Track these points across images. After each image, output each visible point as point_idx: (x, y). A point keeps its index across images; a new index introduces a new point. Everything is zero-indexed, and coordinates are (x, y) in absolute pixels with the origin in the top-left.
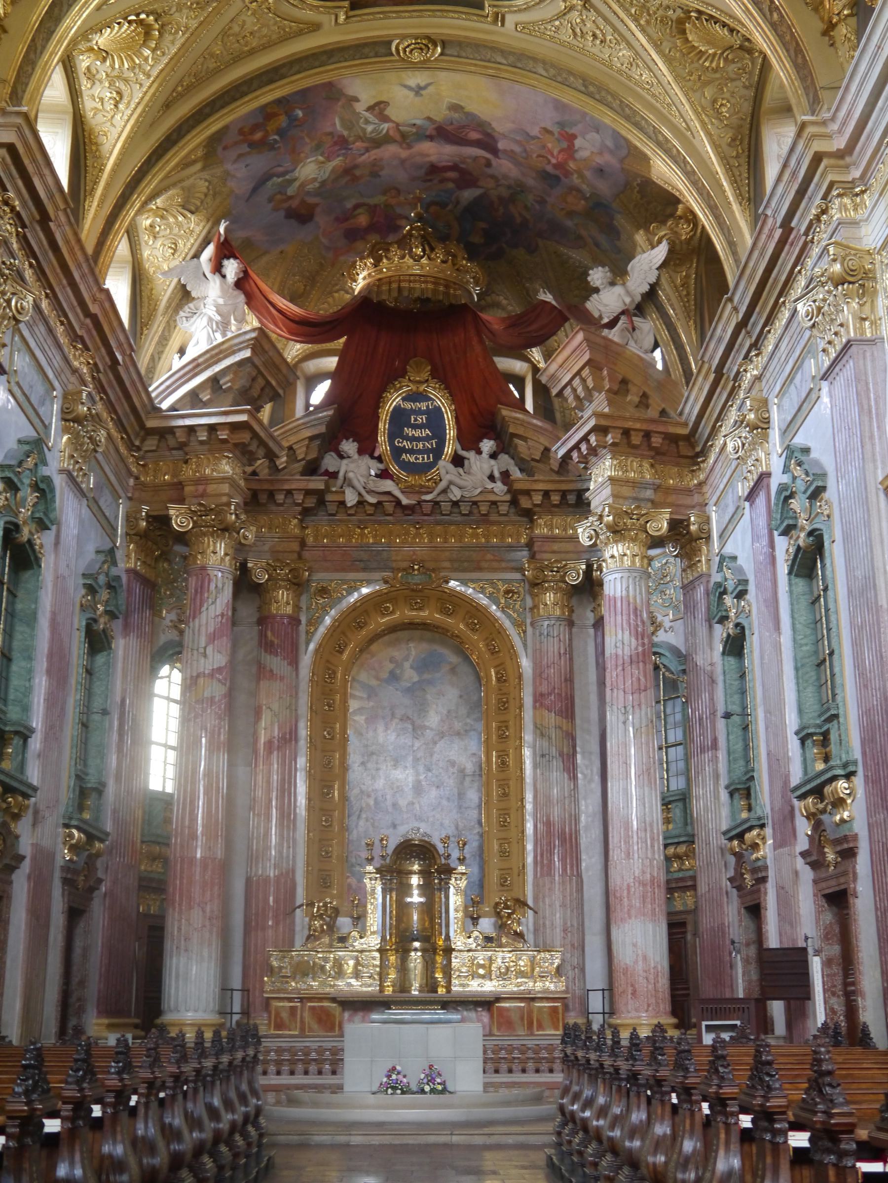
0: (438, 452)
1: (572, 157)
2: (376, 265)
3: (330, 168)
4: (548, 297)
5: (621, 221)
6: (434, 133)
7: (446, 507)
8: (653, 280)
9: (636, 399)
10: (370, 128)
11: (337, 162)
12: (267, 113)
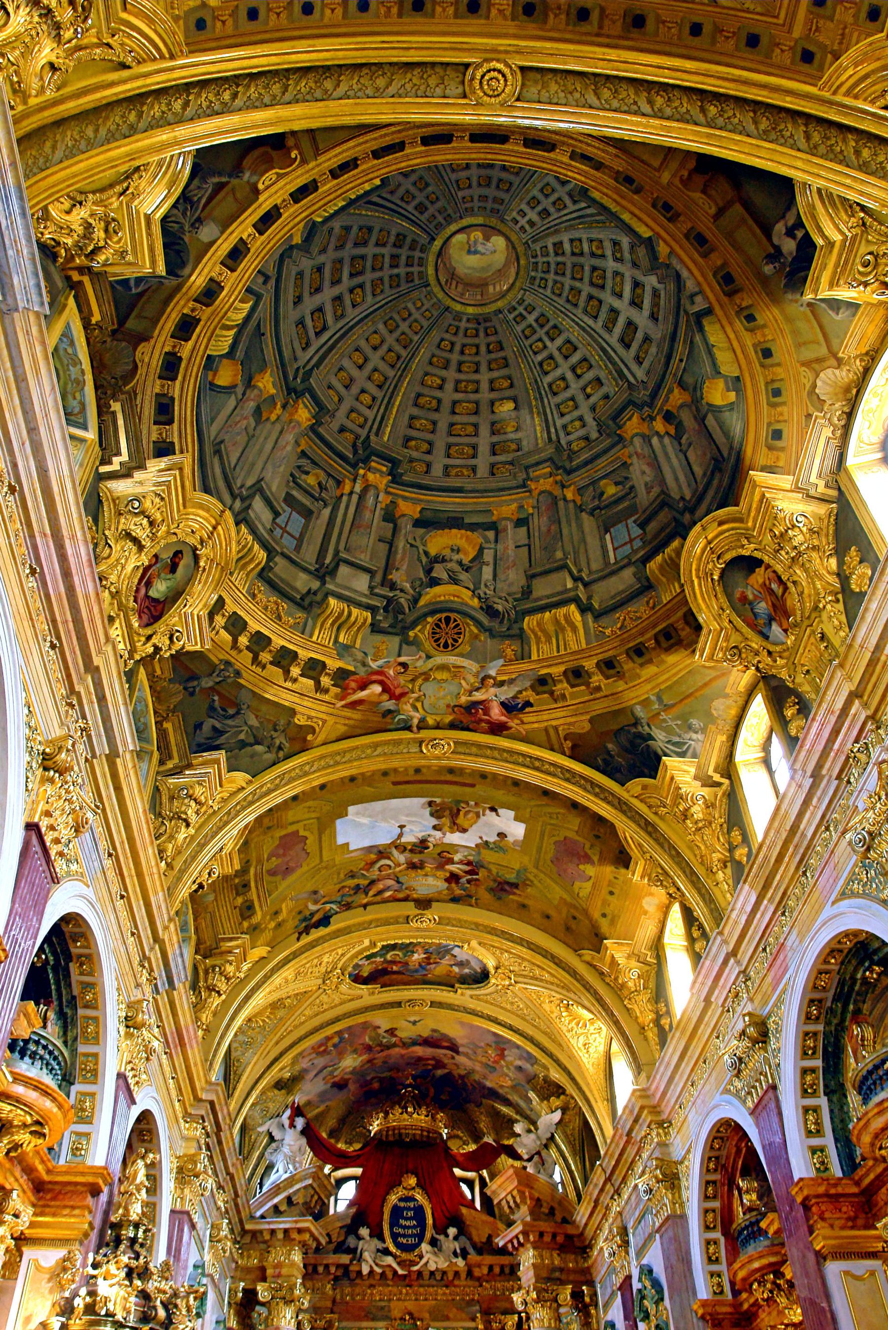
0: (421, 1237)
2: (385, 1117)
7: (426, 1275)
9: (547, 1211)
11: (365, 1057)
12: (328, 1039)
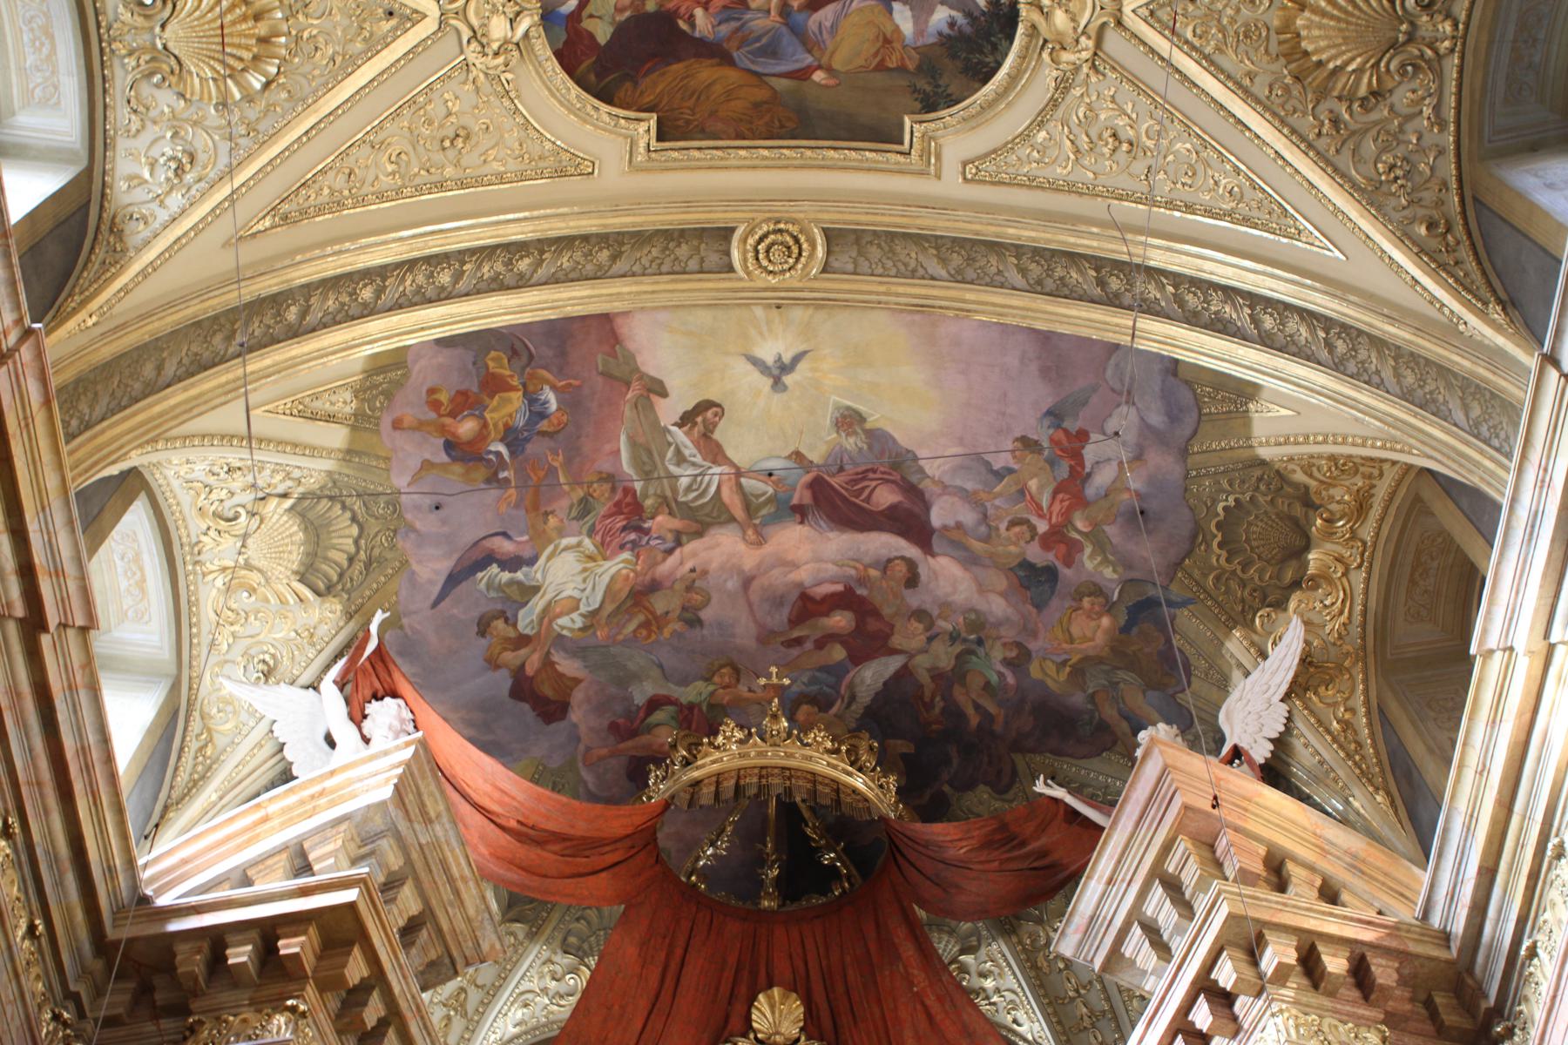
1: (1080, 501)
3: (606, 579)
4: (1059, 793)
5: (1190, 625)
6: (807, 499)
8: (1276, 728)
10: (685, 476)
